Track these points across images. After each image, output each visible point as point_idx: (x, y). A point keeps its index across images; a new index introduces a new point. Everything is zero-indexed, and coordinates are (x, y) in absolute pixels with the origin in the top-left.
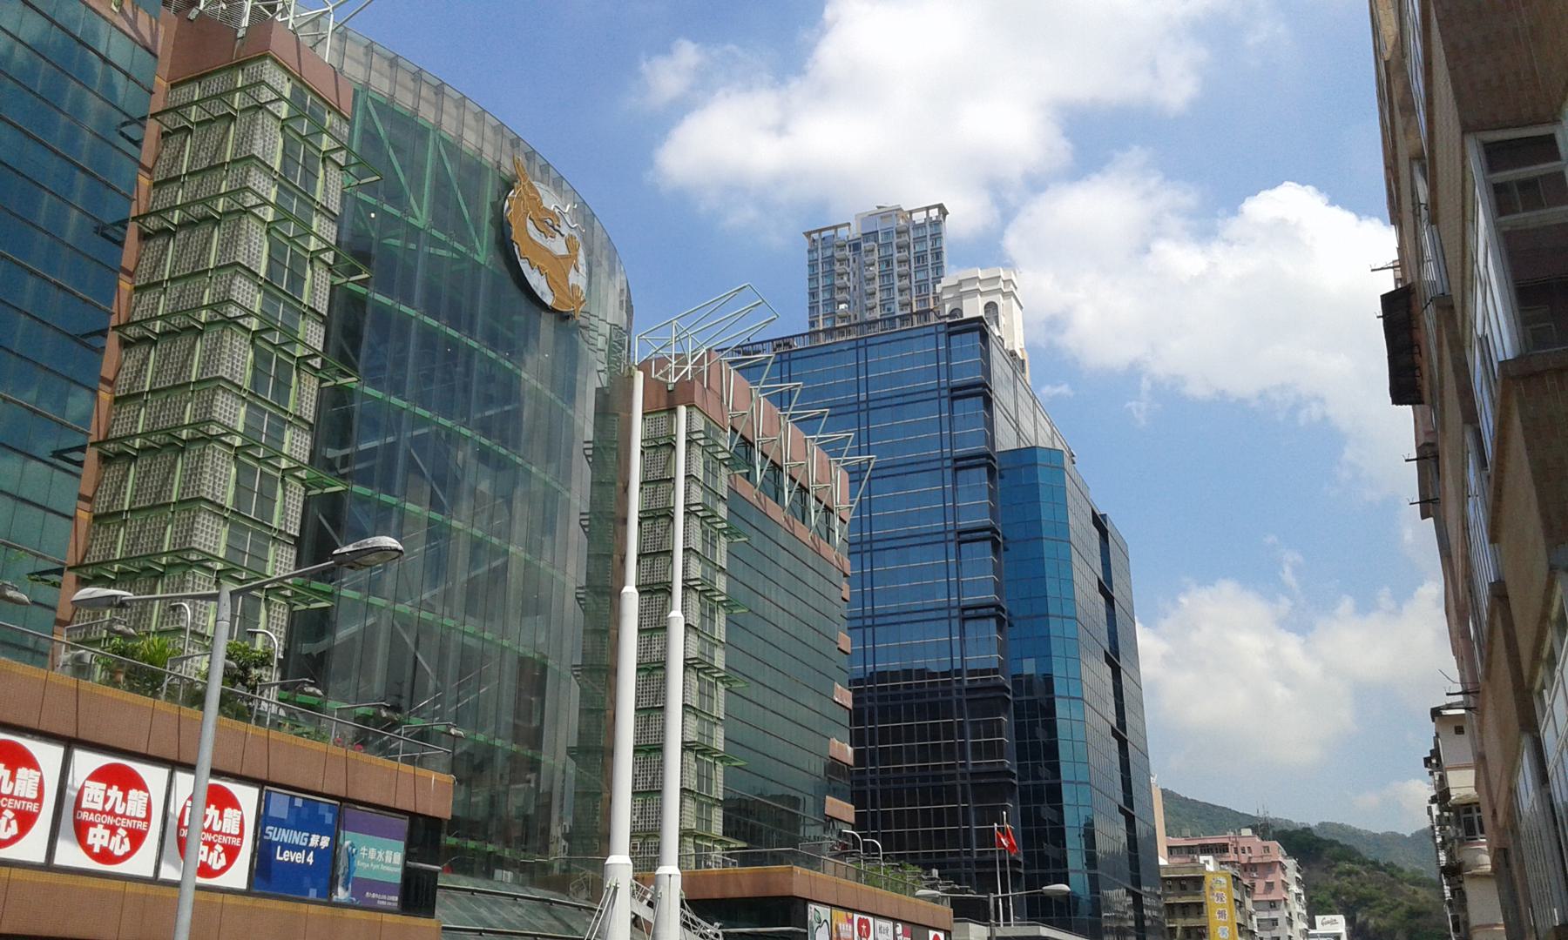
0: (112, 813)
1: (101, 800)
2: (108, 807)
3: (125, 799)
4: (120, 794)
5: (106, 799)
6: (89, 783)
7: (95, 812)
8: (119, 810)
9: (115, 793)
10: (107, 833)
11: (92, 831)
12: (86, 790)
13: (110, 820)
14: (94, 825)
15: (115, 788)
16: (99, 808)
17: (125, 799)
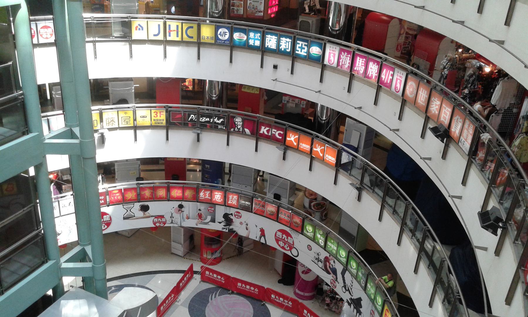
0: (284, 239)
1: (281, 236)
2: (283, 238)
3: (287, 238)
4: (286, 237)
5: (282, 237)
6: (277, 232)
7: (280, 238)
8: (286, 240)
9: (284, 236)
10: (283, 244)
11: (280, 242)
12: (277, 233)
13: (283, 241)
14: (280, 241)
15: (285, 235)
16: (281, 238)
17: (287, 238)
